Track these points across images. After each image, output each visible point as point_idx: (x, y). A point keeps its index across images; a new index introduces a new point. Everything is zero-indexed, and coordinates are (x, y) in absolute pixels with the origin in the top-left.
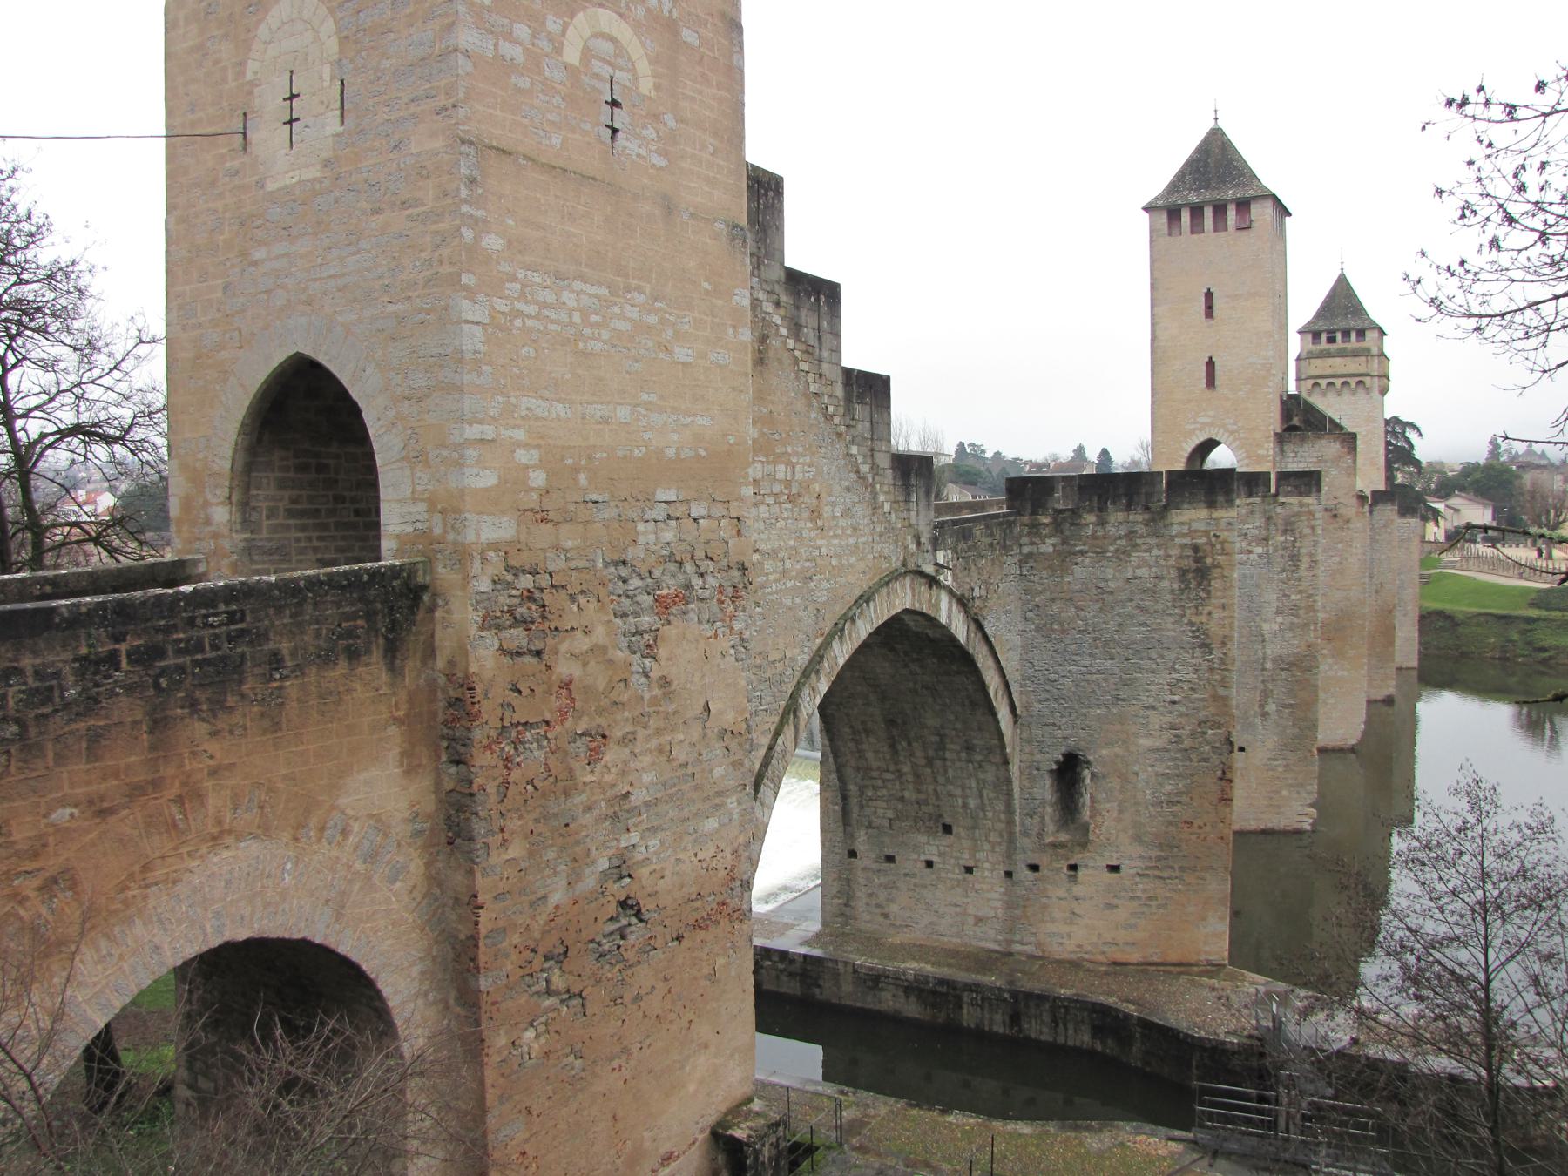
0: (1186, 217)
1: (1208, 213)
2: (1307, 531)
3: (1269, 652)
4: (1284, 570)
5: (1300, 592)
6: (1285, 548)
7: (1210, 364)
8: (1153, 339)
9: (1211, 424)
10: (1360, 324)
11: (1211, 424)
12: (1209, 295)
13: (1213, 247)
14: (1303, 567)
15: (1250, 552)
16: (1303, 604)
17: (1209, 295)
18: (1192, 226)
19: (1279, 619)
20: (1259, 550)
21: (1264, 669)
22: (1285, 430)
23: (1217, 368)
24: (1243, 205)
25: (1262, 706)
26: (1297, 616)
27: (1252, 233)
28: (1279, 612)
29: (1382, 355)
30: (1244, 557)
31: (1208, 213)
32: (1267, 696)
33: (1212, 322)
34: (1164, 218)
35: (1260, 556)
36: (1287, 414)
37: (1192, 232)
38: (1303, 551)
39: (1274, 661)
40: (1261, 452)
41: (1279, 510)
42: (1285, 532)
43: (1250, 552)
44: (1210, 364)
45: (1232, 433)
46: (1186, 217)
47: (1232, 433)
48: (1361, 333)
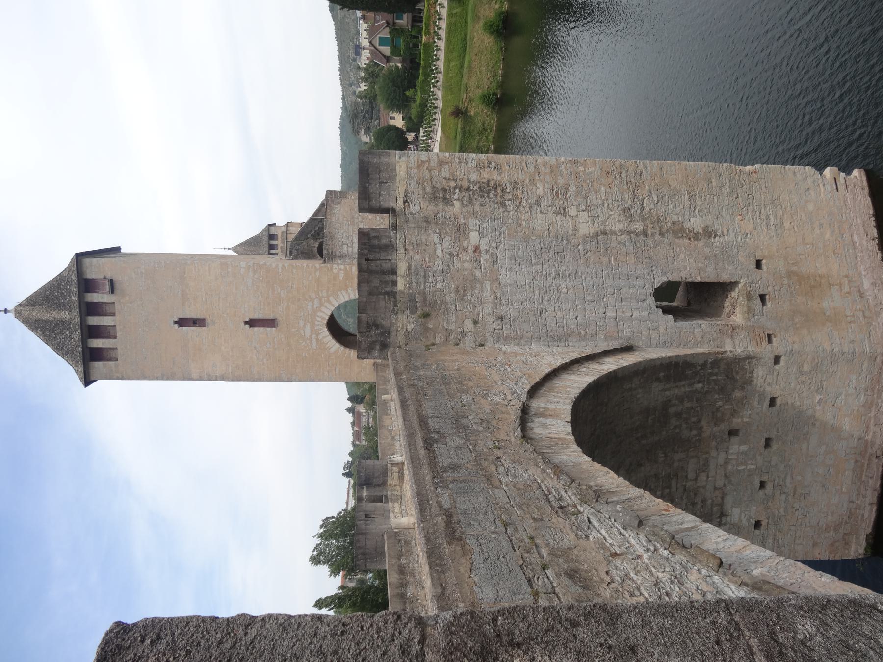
0: (97, 343)
1: (93, 320)
2: (445, 172)
3: (620, 226)
4: (502, 204)
5: (533, 182)
6: (470, 201)
7: (252, 323)
8: (223, 378)
9: (313, 325)
10: (266, 238)
11: (313, 325)
12: (181, 322)
13: (127, 318)
14: (496, 177)
15: (477, 249)
16: (548, 178)
17: (181, 322)
18: (108, 337)
19: (573, 211)
20: (474, 236)
21: (645, 233)
22: (321, 254)
23: (256, 316)
24: (87, 285)
25: (696, 237)
26: (567, 188)
27: (117, 278)
28: (563, 212)
29: (288, 225)
30: (484, 258)
31: (93, 320)
32: (682, 230)
33: (208, 321)
34: (98, 366)
35: (482, 236)
36: (307, 255)
37: (115, 337)
38: (474, 177)
39: (632, 220)
40: (342, 275)
41: (414, 208)
42: (447, 201)
43: (477, 249)
44: (252, 323)
45: (321, 304)
46: (97, 343)
47: (321, 304)
48: (272, 237)
